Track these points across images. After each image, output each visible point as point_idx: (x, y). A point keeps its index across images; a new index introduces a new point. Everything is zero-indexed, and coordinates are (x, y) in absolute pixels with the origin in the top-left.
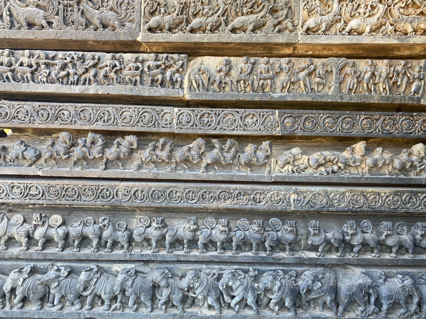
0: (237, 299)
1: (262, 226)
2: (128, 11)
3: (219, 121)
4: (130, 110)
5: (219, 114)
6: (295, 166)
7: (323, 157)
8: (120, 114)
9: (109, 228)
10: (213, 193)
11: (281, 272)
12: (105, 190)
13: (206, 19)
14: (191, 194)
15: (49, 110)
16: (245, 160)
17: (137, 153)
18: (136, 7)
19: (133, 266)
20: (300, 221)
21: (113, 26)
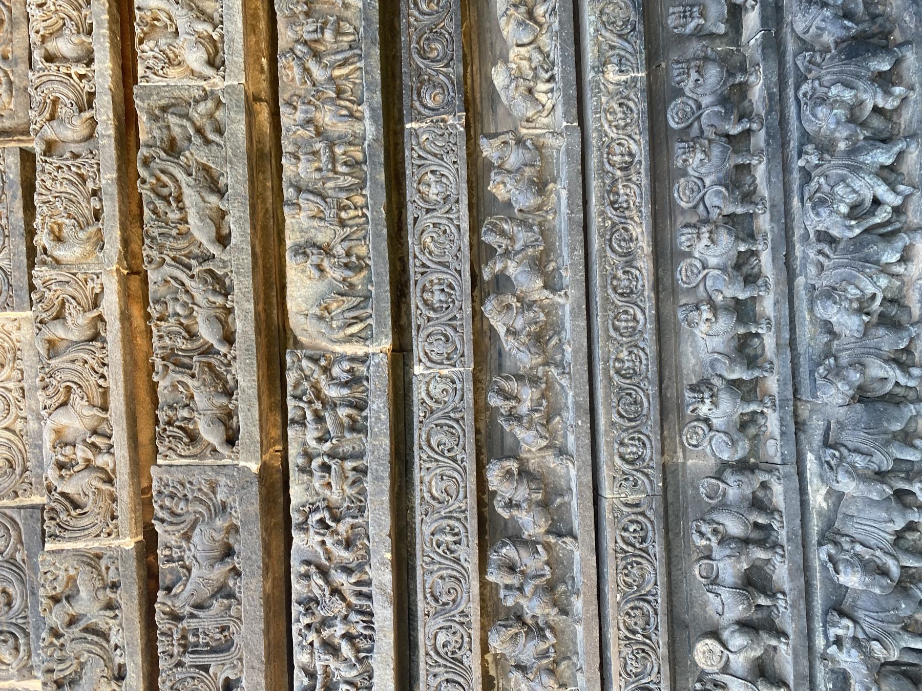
0: (882, 191)
1: (692, 144)
2: (190, 497)
3: (439, 263)
4: (427, 479)
5: (424, 265)
6: (536, 77)
7: (512, 11)
8: (437, 505)
9: (721, 520)
10: (617, 269)
11: (805, 87)
12: (625, 534)
13: (199, 306)
14: (623, 324)
15: (439, 680)
16: (530, 195)
17: (528, 460)
18: (180, 476)
19: (810, 457)
20: (663, 65)
21: (228, 532)
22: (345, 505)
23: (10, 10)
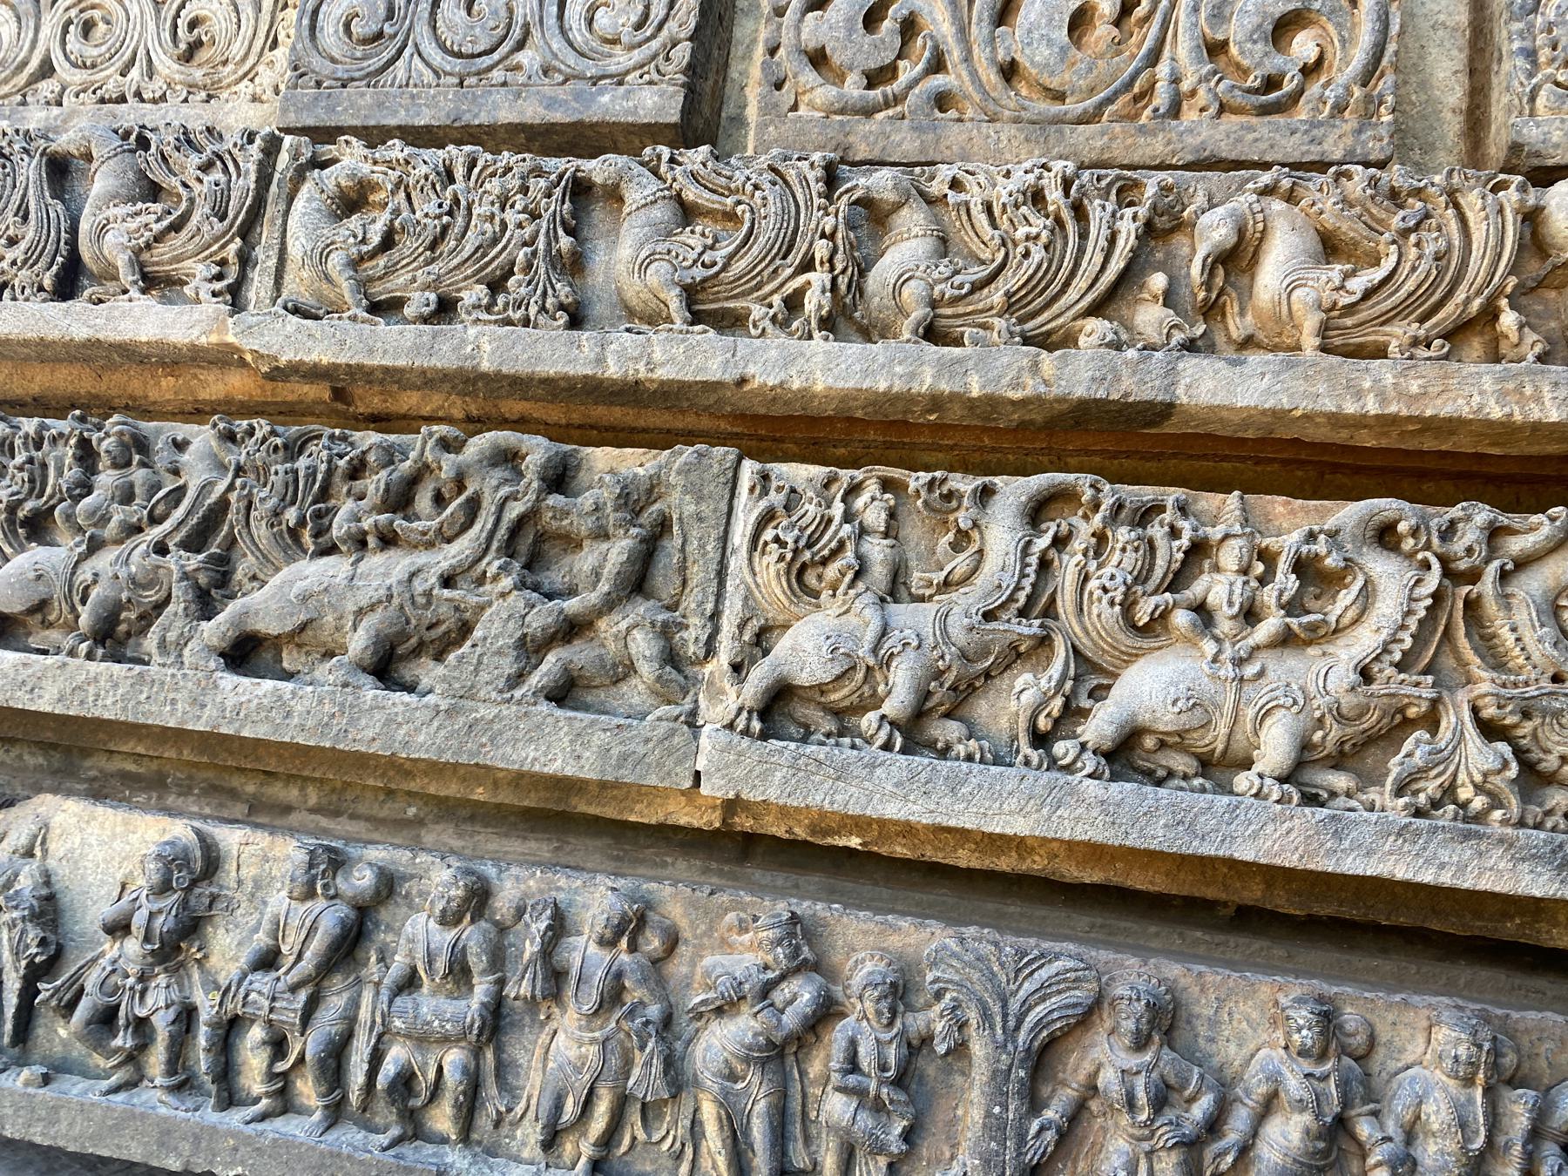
13: (83, 558)
23: (1084, 119)
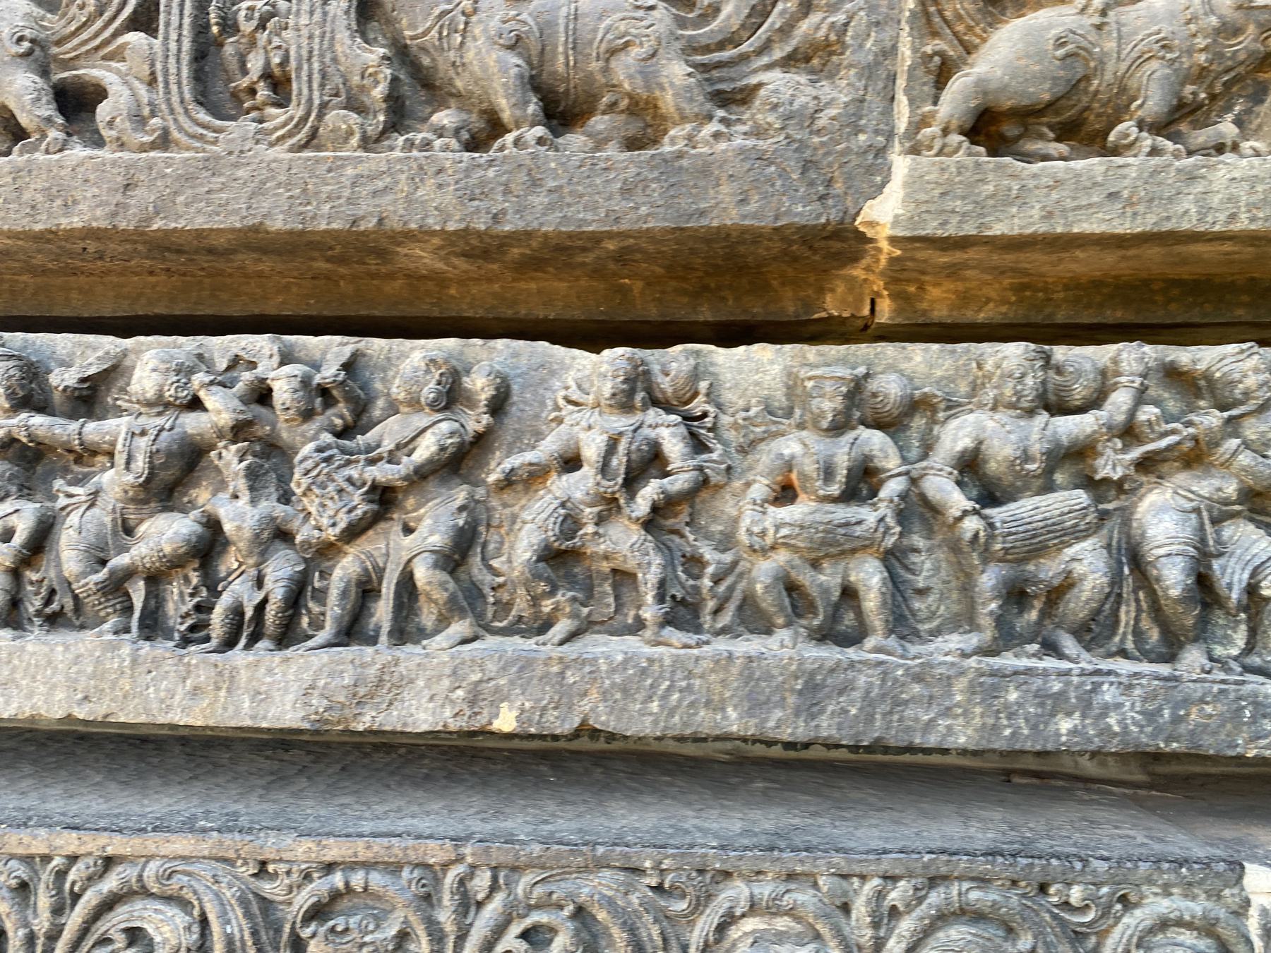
4: (802, 897)
22: (708, 553)
